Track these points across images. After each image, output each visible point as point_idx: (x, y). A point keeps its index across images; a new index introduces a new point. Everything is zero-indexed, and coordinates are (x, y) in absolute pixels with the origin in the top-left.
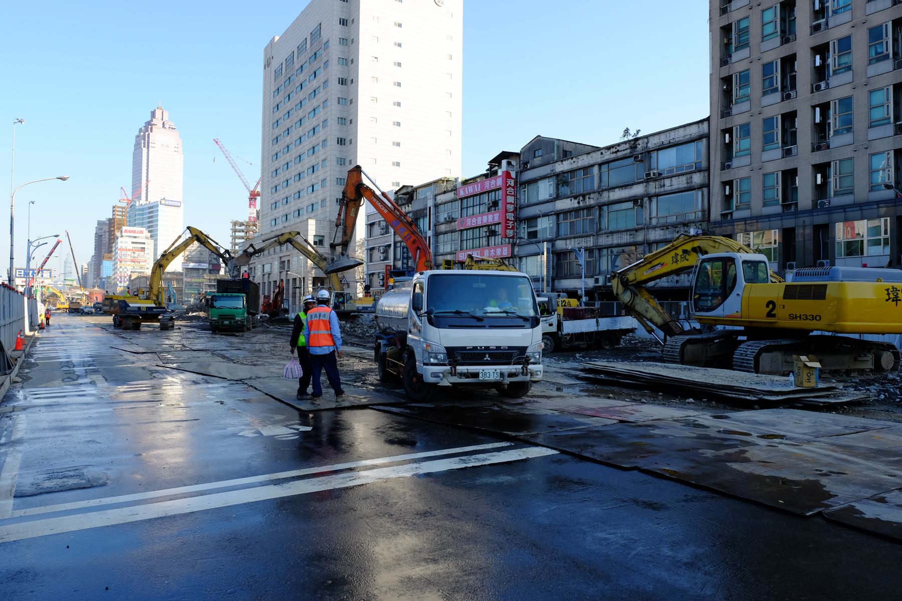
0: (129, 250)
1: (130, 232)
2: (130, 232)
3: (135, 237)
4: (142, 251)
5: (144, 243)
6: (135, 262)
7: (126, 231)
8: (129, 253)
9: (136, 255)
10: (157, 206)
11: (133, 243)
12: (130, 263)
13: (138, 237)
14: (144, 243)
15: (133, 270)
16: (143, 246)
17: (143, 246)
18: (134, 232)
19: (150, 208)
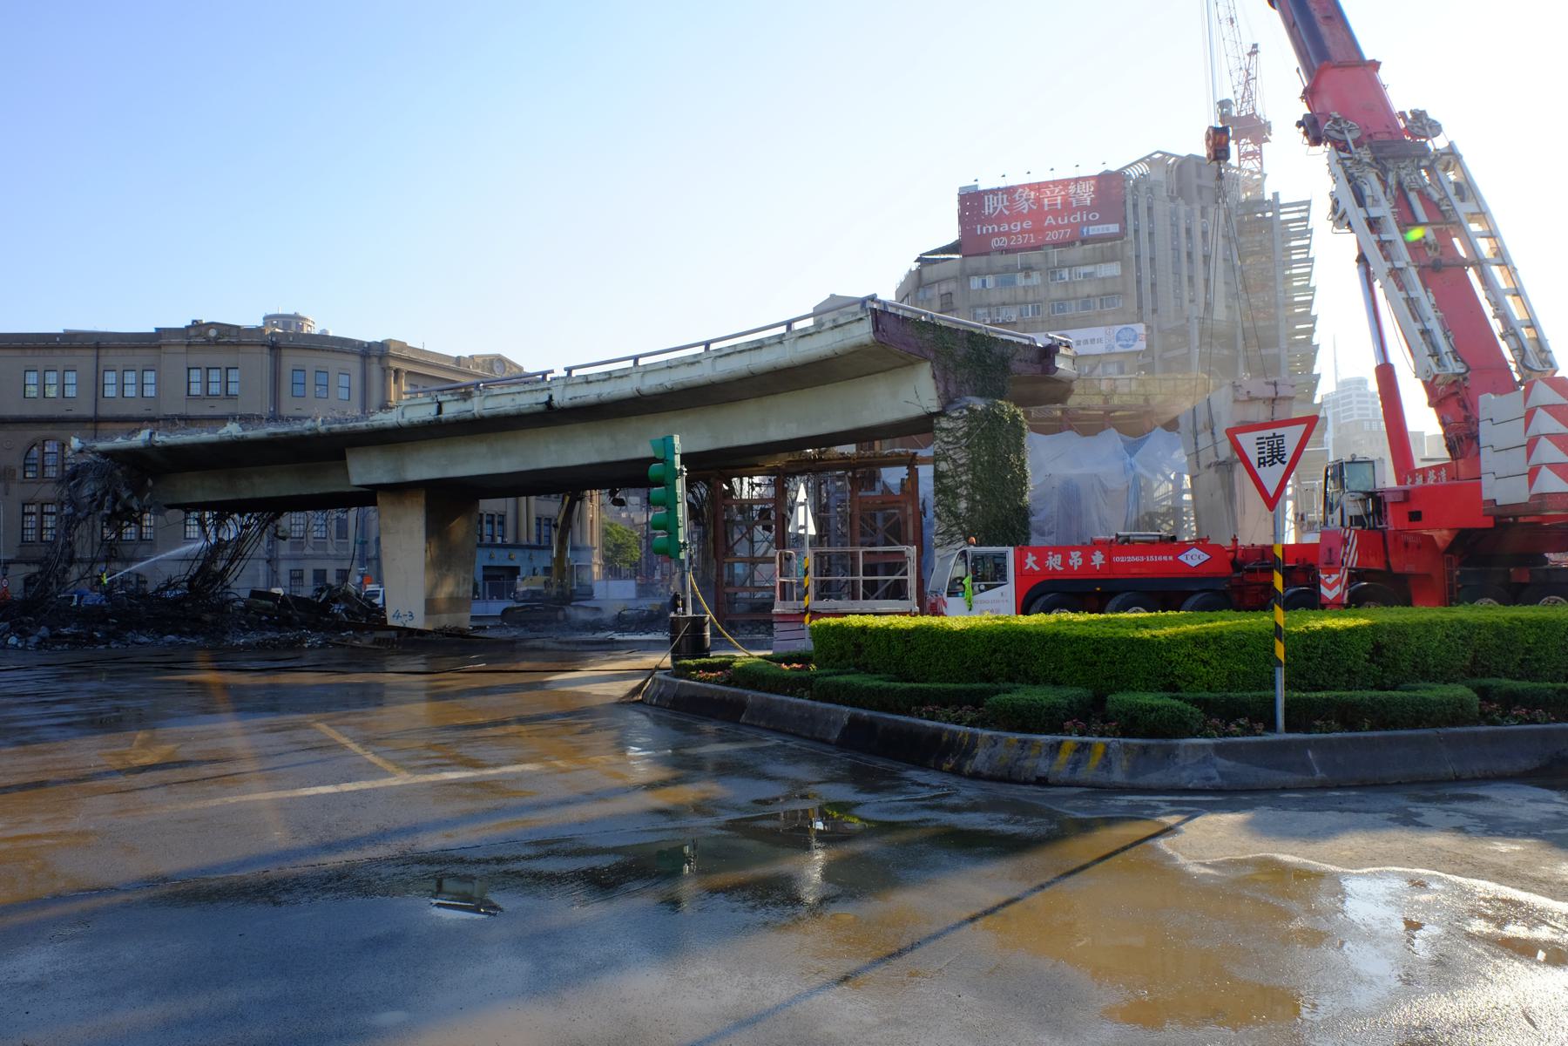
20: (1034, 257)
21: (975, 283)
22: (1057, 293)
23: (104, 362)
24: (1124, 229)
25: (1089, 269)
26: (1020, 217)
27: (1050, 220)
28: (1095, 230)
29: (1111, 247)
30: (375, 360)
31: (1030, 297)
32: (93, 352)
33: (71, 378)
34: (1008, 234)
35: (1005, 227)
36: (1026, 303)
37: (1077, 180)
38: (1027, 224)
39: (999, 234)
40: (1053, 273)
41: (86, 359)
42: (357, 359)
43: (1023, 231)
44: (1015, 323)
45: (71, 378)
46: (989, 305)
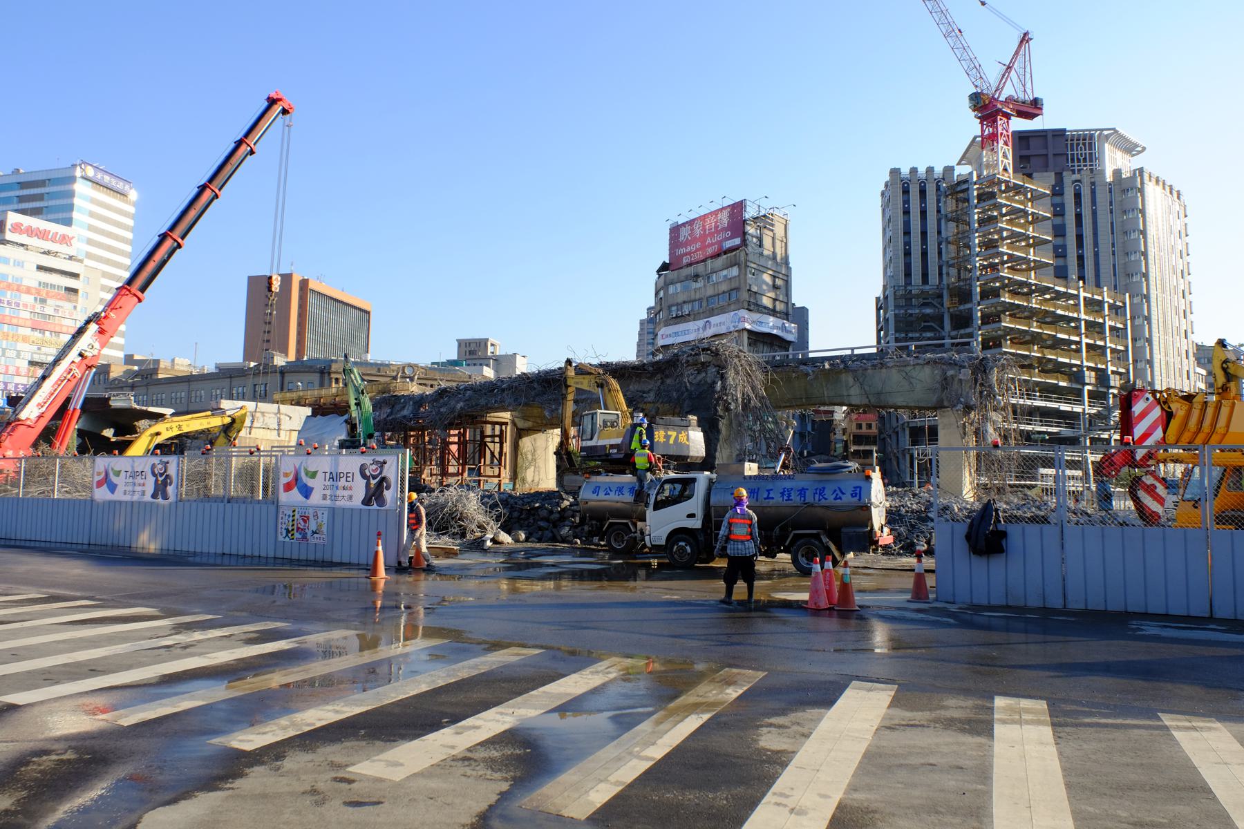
0: (28, 291)
1: (30, 232)
2: (30, 232)
3: (47, 253)
4: (70, 301)
5: (75, 276)
6: (42, 331)
7: (17, 228)
8: (28, 299)
9: (49, 310)
10: (72, 179)
11: (40, 268)
12: (28, 332)
13: (56, 254)
14: (75, 276)
15: (37, 358)
16: (72, 283)
17: (72, 283)
18: (43, 235)
19: (23, 185)
20: (700, 268)
21: (671, 289)
22: (710, 292)
23: (233, 384)
24: (744, 242)
25: (725, 272)
26: (695, 240)
27: (709, 241)
28: (728, 244)
29: (735, 255)
30: (326, 375)
31: (697, 297)
32: (229, 380)
33: (183, 394)
34: (689, 253)
35: (689, 249)
36: (695, 300)
37: (715, 213)
38: (698, 245)
39: (686, 254)
40: (709, 278)
41: (184, 386)
42: (318, 375)
43: (697, 250)
44: (689, 315)
45: (183, 394)
46: (677, 304)
